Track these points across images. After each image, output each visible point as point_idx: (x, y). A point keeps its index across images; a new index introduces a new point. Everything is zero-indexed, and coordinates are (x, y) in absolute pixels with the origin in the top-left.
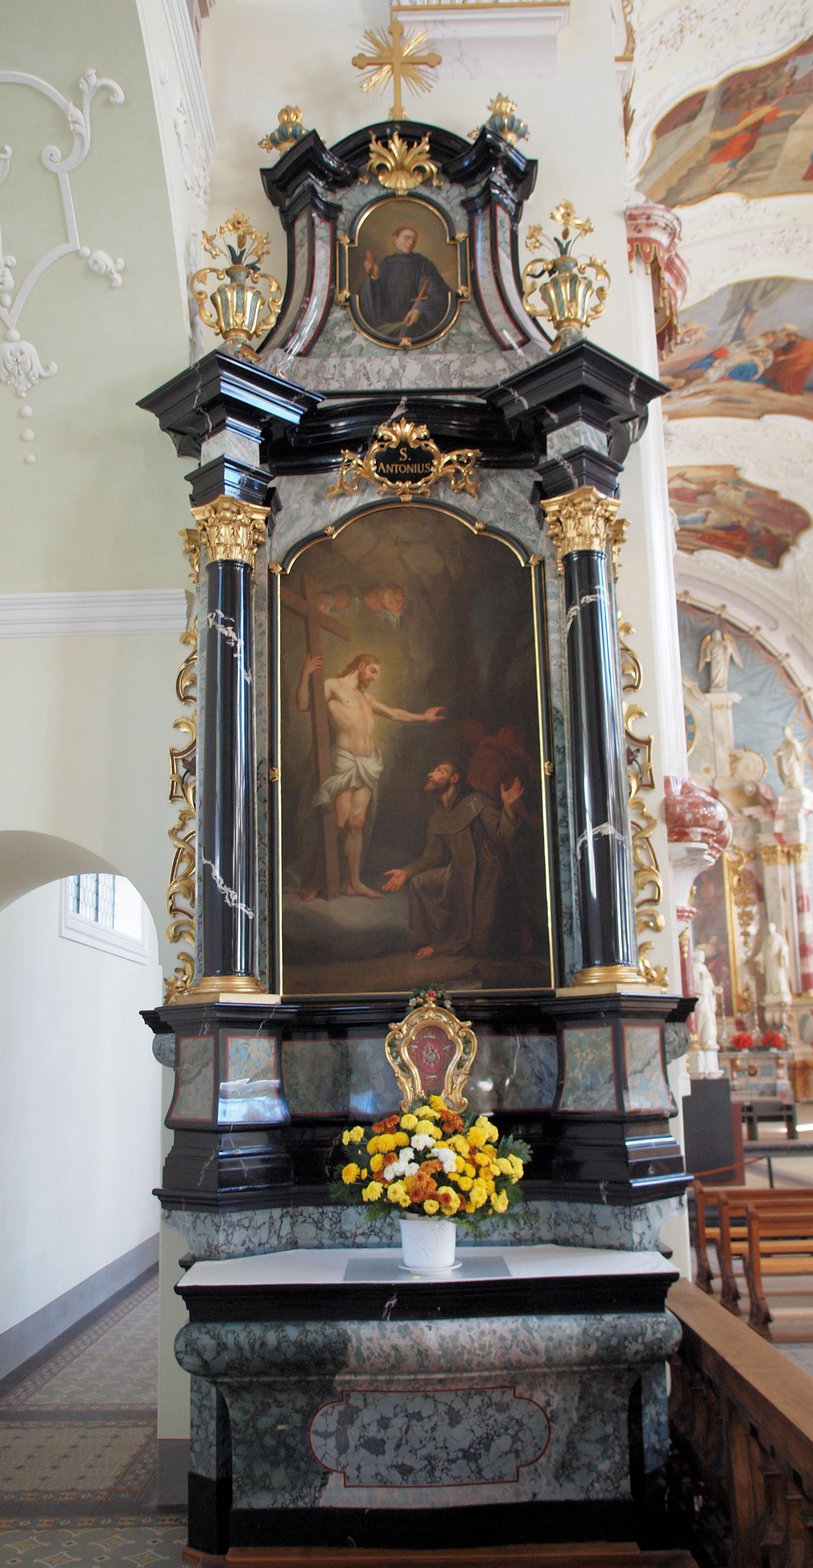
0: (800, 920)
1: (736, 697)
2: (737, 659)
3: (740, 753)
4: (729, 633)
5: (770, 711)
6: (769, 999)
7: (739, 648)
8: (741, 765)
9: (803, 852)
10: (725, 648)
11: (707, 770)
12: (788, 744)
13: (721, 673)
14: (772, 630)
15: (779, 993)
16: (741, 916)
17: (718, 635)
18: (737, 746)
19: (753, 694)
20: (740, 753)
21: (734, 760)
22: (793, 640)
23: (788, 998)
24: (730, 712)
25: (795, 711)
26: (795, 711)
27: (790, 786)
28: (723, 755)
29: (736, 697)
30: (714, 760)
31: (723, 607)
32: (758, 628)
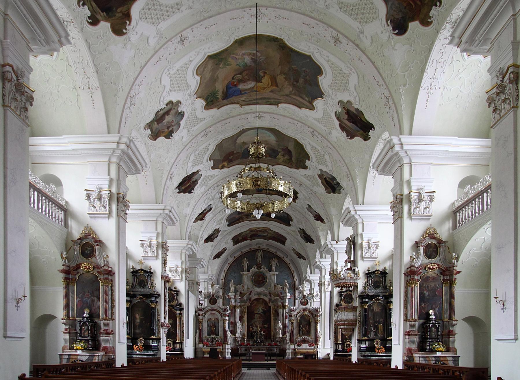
0: (285, 320)
1: (277, 273)
2: (278, 264)
3: (276, 285)
4: (277, 258)
5: (284, 276)
6: (278, 336)
7: (278, 262)
8: (276, 288)
9: (287, 307)
10: (275, 262)
11: (269, 288)
12: (286, 284)
13: (274, 267)
14: (286, 257)
15: (279, 335)
16: (274, 319)
17: (274, 259)
18: (276, 284)
19: (281, 272)
20: (276, 285)
21: (275, 286)
22: (291, 260)
23: (281, 336)
24: (275, 276)
25: (290, 276)
26: (290, 276)
27: (285, 293)
28: (273, 285)
29: (277, 273)
30: (271, 286)
31: (276, 252)
32: (283, 257)
